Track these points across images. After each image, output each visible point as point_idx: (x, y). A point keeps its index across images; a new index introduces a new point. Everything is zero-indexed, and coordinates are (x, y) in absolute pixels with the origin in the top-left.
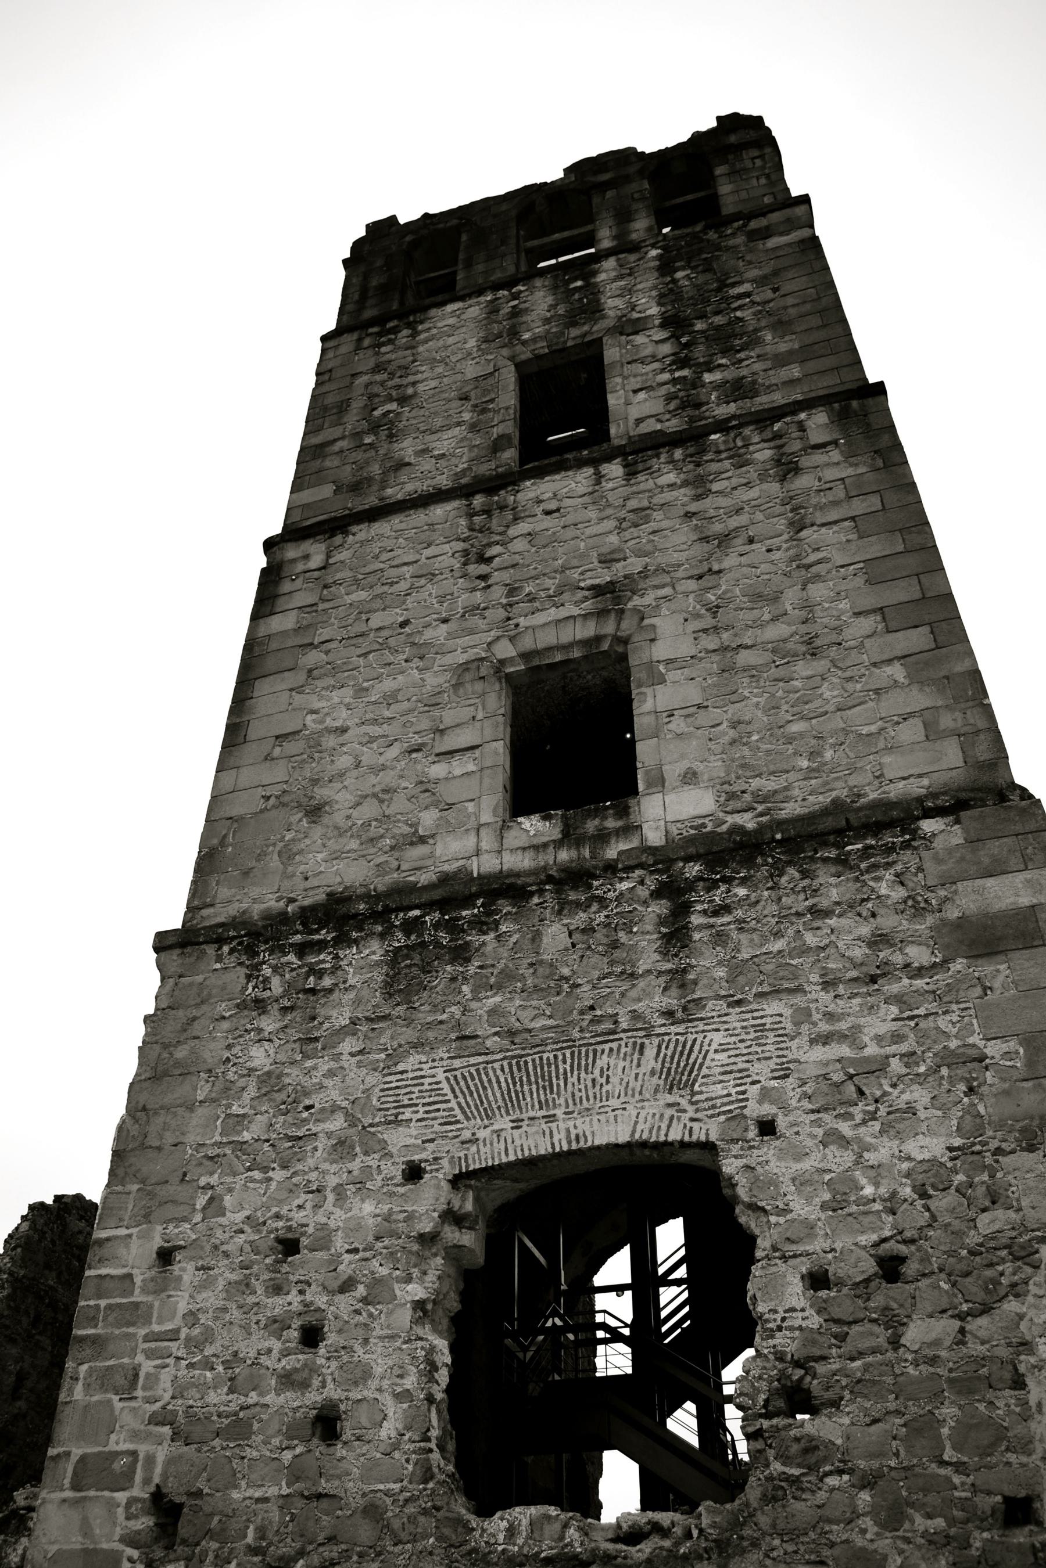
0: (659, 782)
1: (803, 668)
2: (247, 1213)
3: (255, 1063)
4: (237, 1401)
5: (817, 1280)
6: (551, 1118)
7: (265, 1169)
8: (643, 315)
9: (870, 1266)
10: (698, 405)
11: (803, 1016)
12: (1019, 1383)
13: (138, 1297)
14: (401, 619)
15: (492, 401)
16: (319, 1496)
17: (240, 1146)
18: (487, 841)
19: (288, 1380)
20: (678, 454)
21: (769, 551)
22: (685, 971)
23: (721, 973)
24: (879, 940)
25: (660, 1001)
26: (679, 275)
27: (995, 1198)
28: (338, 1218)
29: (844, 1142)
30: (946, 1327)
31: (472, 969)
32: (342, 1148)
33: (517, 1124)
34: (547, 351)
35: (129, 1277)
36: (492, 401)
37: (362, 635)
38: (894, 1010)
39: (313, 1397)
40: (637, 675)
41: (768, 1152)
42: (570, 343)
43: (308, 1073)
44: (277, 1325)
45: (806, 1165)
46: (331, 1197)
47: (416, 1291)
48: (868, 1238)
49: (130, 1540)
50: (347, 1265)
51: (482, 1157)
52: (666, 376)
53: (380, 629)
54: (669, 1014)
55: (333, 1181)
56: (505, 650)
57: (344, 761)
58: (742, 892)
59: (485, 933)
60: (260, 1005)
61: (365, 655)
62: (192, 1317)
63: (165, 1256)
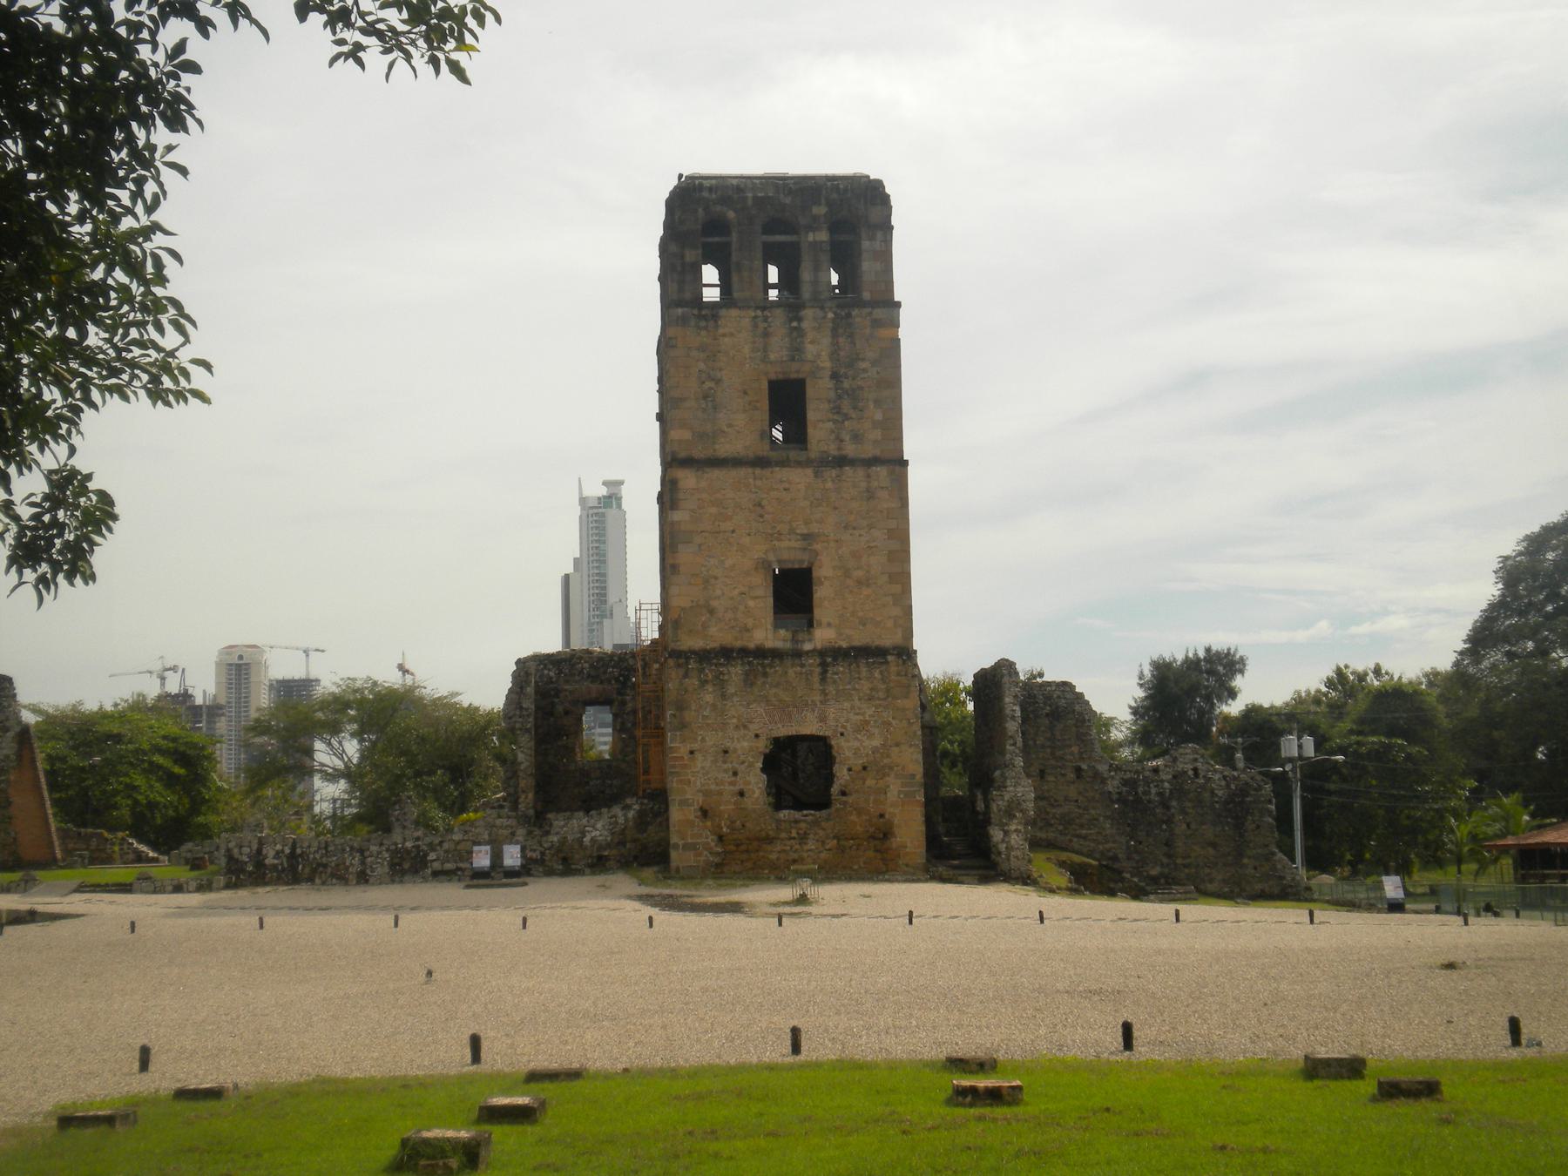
0: (820, 624)
1: (866, 591)
2: (712, 743)
3: (708, 700)
4: (718, 788)
5: (850, 770)
6: (792, 726)
7: (716, 731)
8: (822, 365)
9: (861, 768)
10: (842, 441)
11: (853, 708)
12: (886, 793)
13: (686, 762)
14: (732, 528)
15: (757, 401)
16: (741, 809)
17: (708, 725)
18: (770, 636)
19: (732, 784)
20: (834, 473)
21: (860, 535)
22: (824, 690)
23: (834, 692)
24: (872, 689)
25: (817, 698)
26: (841, 340)
27: (888, 756)
28: (738, 746)
29: (859, 740)
30: (874, 782)
31: (769, 680)
32: (737, 727)
33: (783, 726)
34: (781, 377)
35: (683, 757)
36: (757, 401)
37: (719, 532)
38: (874, 709)
39: (737, 788)
40: (815, 581)
41: (842, 739)
42: (794, 376)
43: (725, 705)
44: (726, 771)
45: (850, 744)
46: (736, 740)
47: (760, 765)
48: (861, 762)
49: (696, 817)
50: (742, 758)
51: (776, 734)
52: (831, 416)
53: (725, 532)
54: (821, 702)
55: (736, 736)
56: (771, 557)
57: (718, 592)
58: (841, 669)
59: (771, 669)
60: (706, 681)
61: (720, 544)
62: (703, 768)
63: (692, 752)
